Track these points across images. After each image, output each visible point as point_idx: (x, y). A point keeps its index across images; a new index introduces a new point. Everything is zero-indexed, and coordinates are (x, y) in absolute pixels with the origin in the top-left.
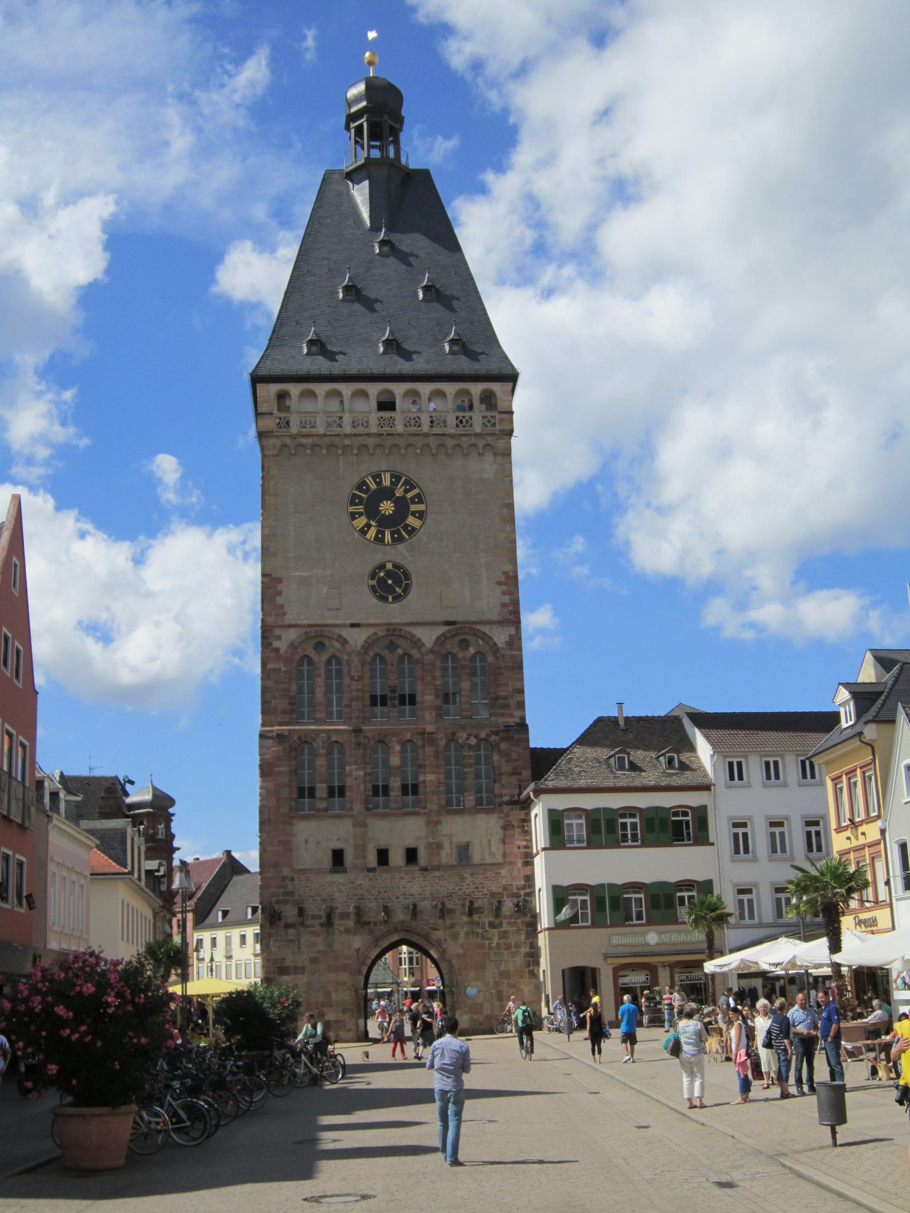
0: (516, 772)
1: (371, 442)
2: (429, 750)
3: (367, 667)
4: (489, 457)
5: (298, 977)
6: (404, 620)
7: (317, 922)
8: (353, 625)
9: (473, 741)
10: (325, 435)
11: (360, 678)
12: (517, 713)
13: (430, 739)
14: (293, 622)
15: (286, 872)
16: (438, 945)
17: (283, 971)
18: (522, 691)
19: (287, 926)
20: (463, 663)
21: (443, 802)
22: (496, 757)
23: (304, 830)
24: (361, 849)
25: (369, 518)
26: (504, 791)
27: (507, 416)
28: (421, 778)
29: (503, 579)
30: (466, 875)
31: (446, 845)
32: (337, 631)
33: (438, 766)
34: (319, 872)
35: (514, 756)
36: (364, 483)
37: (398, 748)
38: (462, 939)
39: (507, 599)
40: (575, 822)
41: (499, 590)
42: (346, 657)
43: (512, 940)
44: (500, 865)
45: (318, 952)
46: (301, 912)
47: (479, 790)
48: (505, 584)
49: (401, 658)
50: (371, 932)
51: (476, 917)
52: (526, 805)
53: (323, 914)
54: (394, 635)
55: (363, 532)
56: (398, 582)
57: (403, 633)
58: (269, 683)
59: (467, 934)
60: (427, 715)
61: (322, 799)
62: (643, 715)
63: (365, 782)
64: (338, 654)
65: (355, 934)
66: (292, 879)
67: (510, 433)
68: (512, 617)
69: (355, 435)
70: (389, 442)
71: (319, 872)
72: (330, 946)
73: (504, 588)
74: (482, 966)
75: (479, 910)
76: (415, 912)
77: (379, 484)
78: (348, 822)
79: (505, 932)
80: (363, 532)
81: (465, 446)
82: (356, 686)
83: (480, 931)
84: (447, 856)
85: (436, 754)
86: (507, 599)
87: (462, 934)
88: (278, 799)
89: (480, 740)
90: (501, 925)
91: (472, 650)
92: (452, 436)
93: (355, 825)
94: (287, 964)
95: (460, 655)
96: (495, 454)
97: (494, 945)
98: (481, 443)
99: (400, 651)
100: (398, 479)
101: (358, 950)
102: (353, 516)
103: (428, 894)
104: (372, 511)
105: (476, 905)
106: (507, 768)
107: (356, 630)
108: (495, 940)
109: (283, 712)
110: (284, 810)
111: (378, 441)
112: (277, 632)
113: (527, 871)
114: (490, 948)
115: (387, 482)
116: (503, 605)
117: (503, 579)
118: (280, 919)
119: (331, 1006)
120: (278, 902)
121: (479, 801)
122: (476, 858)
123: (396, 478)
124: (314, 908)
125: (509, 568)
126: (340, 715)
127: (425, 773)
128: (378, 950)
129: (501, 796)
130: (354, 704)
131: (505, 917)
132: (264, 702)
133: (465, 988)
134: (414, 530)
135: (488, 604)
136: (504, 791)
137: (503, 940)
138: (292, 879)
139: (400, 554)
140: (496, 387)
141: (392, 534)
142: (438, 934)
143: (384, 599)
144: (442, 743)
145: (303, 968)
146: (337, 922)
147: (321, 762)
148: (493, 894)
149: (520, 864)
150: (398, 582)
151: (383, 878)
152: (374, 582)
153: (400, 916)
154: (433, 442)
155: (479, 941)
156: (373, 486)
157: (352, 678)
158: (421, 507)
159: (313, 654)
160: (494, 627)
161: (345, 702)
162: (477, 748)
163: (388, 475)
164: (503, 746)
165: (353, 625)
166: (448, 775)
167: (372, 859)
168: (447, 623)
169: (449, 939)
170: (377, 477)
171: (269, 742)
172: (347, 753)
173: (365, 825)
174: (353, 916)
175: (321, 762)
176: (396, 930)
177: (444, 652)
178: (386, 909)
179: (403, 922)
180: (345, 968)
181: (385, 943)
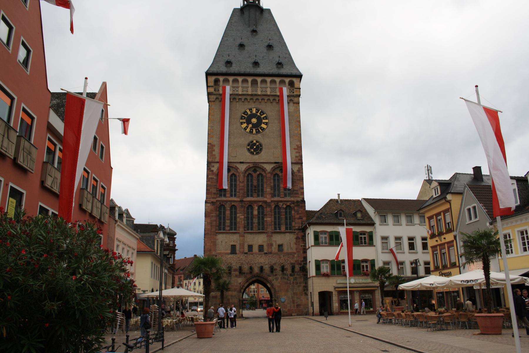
0: (300, 218)
1: (249, 98)
2: (268, 209)
3: (246, 178)
6: (260, 161)
8: (241, 163)
9: (285, 206)
11: (243, 182)
12: (301, 196)
15: (214, 253)
16: (270, 282)
18: (303, 188)
21: (273, 228)
22: (293, 212)
25: (248, 124)
26: (296, 225)
27: (298, 90)
28: (265, 219)
29: (296, 147)
32: (235, 164)
33: (271, 215)
35: (300, 212)
36: (246, 112)
37: (257, 208)
38: (279, 280)
39: (298, 155)
40: (324, 236)
41: (294, 151)
47: (286, 224)
49: (259, 175)
50: (245, 277)
51: (285, 272)
52: (304, 230)
54: (256, 167)
55: (245, 129)
58: (209, 183)
59: (281, 278)
60: (268, 196)
61: (228, 226)
62: (347, 199)
64: (235, 173)
65: (239, 277)
66: (216, 256)
67: (299, 96)
68: (300, 161)
70: (255, 98)
74: (287, 291)
76: (261, 269)
77: (251, 112)
78: (238, 235)
80: (245, 129)
82: (241, 185)
84: (275, 249)
85: (271, 211)
86: (298, 155)
87: (280, 278)
88: (211, 226)
93: (240, 236)
95: (280, 174)
96: (294, 103)
99: (258, 173)
101: (240, 283)
102: (242, 123)
104: (249, 122)
106: (297, 216)
107: (242, 164)
109: (214, 194)
111: (251, 97)
112: (213, 164)
115: (254, 111)
116: (296, 157)
117: (296, 147)
121: (286, 228)
122: (285, 249)
123: (258, 110)
125: (299, 143)
127: (267, 217)
128: (248, 283)
130: (241, 191)
132: (207, 190)
134: (264, 129)
136: (296, 225)
137: (295, 281)
140: (294, 80)
141: (256, 130)
142: (270, 278)
143: (252, 153)
144: (273, 206)
146: (233, 273)
147: (228, 213)
148: (291, 264)
149: (301, 252)
151: (250, 257)
153: (256, 270)
154: (271, 98)
156: (249, 113)
157: (240, 182)
158: (267, 121)
161: (237, 190)
162: (286, 209)
163: (255, 109)
164: (296, 208)
165: (241, 163)
166: (275, 218)
167: (246, 250)
168: (275, 163)
169: (275, 280)
170: (251, 110)
171: (209, 205)
172: (238, 209)
173: (244, 236)
175: (228, 213)
176: (255, 276)
178: (251, 268)
180: (235, 290)
181: (251, 281)
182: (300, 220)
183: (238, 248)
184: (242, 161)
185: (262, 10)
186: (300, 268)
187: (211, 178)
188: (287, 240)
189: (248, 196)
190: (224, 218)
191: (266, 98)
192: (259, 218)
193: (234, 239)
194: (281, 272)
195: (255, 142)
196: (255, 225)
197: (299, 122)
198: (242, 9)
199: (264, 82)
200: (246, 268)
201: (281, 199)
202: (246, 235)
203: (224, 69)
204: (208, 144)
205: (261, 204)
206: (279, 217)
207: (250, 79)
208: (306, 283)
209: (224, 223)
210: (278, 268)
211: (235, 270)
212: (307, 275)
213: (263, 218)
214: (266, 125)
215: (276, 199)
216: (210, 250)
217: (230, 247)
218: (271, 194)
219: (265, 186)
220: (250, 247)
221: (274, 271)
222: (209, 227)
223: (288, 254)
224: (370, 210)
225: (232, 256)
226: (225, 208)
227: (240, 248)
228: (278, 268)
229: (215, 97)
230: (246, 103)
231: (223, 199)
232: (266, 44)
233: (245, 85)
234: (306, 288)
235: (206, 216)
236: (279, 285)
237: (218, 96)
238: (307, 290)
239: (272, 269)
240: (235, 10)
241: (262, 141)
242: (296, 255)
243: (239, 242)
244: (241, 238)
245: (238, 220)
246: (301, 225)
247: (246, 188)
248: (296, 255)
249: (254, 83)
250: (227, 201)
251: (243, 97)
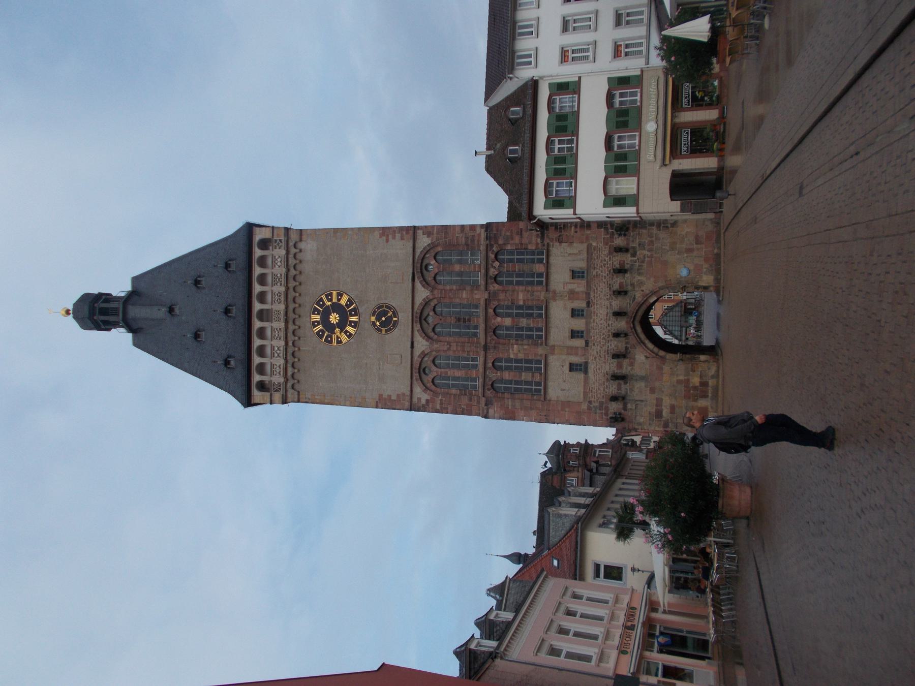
0: (520, 233)
1: (291, 327)
2: (502, 296)
4: (302, 245)
5: (664, 404)
7: (623, 386)
8: (412, 347)
9: (497, 264)
10: (286, 359)
11: (449, 343)
12: (478, 230)
13: (492, 296)
14: (409, 389)
15: (584, 406)
17: (659, 414)
18: (463, 227)
19: (625, 408)
20: (441, 269)
21: (539, 288)
22: (509, 247)
23: (554, 392)
24: (571, 350)
28: (521, 303)
30: (594, 273)
31: (571, 287)
32: (416, 358)
33: (513, 291)
34: (586, 380)
35: (508, 234)
36: (318, 333)
37: (499, 319)
39: (398, 236)
42: (434, 353)
43: (646, 240)
44: (589, 247)
45: (646, 386)
46: (614, 399)
47: (533, 261)
48: (388, 236)
50: (634, 347)
51: (627, 267)
52: (542, 226)
53: (617, 381)
54: (420, 318)
55: (350, 336)
56: (385, 313)
57: (419, 311)
58: (450, 408)
59: (639, 274)
60: (477, 296)
61: (533, 376)
63: (522, 345)
64: (431, 359)
65: (634, 359)
66: (590, 402)
67: (287, 230)
68: (411, 232)
69: (286, 338)
70: (291, 315)
71: (586, 380)
72: (642, 378)
73: (390, 237)
74: (665, 263)
75: (622, 264)
76: (618, 314)
78: (551, 358)
79: (639, 245)
80: (350, 336)
81: (295, 262)
82: (454, 347)
83: (637, 264)
84: (579, 286)
85: (505, 291)
86: (398, 236)
88: (531, 409)
89: (496, 258)
90: (634, 248)
91: (433, 262)
92: (288, 270)
93: (553, 354)
94: (654, 410)
96: (301, 240)
97: (649, 254)
98: (293, 251)
100: (315, 309)
101: (646, 357)
102: (339, 342)
103: (607, 303)
105: (618, 266)
106: (517, 240)
107: (415, 344)
108: (646, 252)
110: (539, 404)
111: (291, 323)
112: (415, 400)
113: (594, 226)
114: (652, 256)
115: (317, 318)
116: (402, 239)
118: (620, 414)
119: (688, 380)
120: (606, 414)
121: (540, 261)
122: (581, 264)
123: (315, 311)
124: (613, 388)
125: (377, 233)
126: (473, 360)
129: (537, 244)
131: (628, 244)
132: (463, 413)
133: (681, 277)
134: (349, 300)
135: (401, 250)
136: (534, 240)
138: (590, 402)
139: (366, 309)
142: (639, 296)
143: (396, 323)
144: (497, 286)
145: (657, 399)
147: (507, 375)
148: (610, 253)
149: (588, 232)
150: (385, 313)
152: (384, 332)
153: (622, 324)
155: (645, 265)
156: (320, 327)
157: (449, 349)
158: (335, 293)
159: (431, 376)
160: (417, 245)
162: (502, 262)
163: (313, 316)
164: (501, 242)
165: (412, 347)
166: (519, 283)
167: (579, 343)
170: (314, 324)
171: (491, 411)
172: (501, 356)
173: (554, 346)
174: (620, 360)
176: (634, 327)
177: (433, 283)
178: (616, 335)
179: (627, 322)
180: (660, 369)
181: (643, 336)
182: (524, 233)
183: (575, 359)
184: (409, 346)
185: (133, 295)
186: (620, 235)
187: (441, 404)
188: (563, 260)
189: (476, 335)
190: (517, 383)
191: (292, 294)
192: (518, 315)
193: (558, 366)
194: (627, 275)
195: (373, 319)
196: (531, 323)
197: (336, 231)
199: (262, 297)
200: (617, 345)
201: (483, 271)
202: (551, 342)
203: (240, 372)
204: (377, 407)
205: (491, 311)
206: (518, 276)
207: (257, 324)
208: (652, 224)
209: (527, 383)
210: (617, 281)
211: (620, 366)
212: (635, 222)
213: (519, 307)
214: (341, 295)
215: (481, 280)
216: (579, 413)
217: (573, 373)
218: (472, 291)
219: (457, 301)
220: (574, 334)
221: (625, 289)
222: (534, 413)
223: (589, 259)
224: (507, 88)
225: (590, 371)
226: (500, 381)
227: (576, 354)
228: (617, 281)
229: (290, 391)
230: (300, 332)
231: (479, 383)
232: (194, 288)
233: (268, 332)
234: (662, 224)
235: (513, 418)
236: (652, 279)
237: (289, 384)
238: (665, 221)
239: (621, 292)
240: (136, 344)
241: (373, 305)
242: (594, 244)
243: (564, 357)
244: (556, 352)
245: (521, 356)
246: (534, 233)
247: (461, 339)
248: (594, 244)
249: (262, 315)
250: (485, 376)
251: (291, 338)
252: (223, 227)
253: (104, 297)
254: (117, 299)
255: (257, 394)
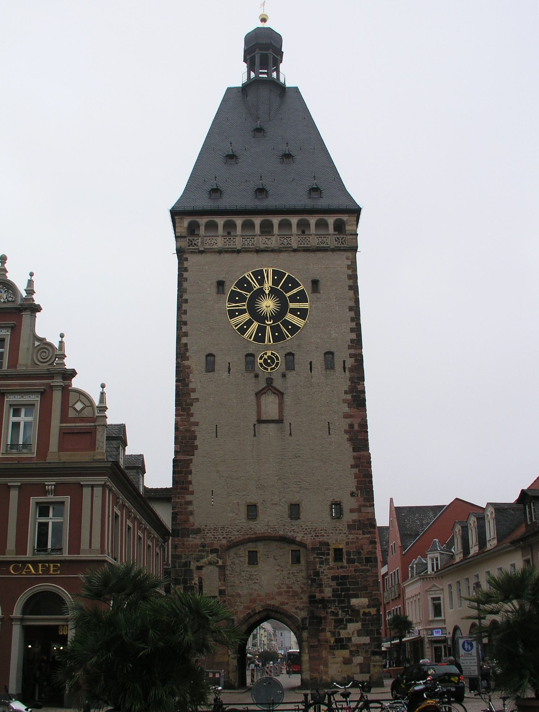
140: (345, 218)
198: (245, 88)
207: (257, 221)
252: (356, 186)
253: (279, 58)
254: (278, 71)
255: (186, 222)
